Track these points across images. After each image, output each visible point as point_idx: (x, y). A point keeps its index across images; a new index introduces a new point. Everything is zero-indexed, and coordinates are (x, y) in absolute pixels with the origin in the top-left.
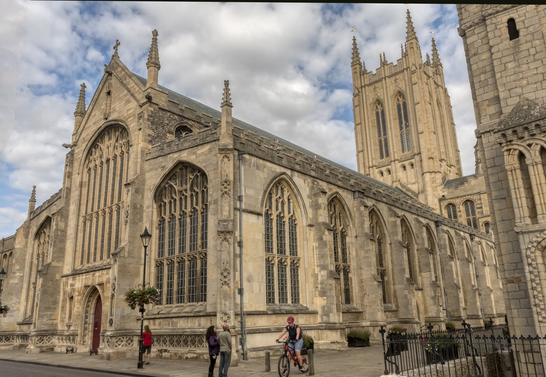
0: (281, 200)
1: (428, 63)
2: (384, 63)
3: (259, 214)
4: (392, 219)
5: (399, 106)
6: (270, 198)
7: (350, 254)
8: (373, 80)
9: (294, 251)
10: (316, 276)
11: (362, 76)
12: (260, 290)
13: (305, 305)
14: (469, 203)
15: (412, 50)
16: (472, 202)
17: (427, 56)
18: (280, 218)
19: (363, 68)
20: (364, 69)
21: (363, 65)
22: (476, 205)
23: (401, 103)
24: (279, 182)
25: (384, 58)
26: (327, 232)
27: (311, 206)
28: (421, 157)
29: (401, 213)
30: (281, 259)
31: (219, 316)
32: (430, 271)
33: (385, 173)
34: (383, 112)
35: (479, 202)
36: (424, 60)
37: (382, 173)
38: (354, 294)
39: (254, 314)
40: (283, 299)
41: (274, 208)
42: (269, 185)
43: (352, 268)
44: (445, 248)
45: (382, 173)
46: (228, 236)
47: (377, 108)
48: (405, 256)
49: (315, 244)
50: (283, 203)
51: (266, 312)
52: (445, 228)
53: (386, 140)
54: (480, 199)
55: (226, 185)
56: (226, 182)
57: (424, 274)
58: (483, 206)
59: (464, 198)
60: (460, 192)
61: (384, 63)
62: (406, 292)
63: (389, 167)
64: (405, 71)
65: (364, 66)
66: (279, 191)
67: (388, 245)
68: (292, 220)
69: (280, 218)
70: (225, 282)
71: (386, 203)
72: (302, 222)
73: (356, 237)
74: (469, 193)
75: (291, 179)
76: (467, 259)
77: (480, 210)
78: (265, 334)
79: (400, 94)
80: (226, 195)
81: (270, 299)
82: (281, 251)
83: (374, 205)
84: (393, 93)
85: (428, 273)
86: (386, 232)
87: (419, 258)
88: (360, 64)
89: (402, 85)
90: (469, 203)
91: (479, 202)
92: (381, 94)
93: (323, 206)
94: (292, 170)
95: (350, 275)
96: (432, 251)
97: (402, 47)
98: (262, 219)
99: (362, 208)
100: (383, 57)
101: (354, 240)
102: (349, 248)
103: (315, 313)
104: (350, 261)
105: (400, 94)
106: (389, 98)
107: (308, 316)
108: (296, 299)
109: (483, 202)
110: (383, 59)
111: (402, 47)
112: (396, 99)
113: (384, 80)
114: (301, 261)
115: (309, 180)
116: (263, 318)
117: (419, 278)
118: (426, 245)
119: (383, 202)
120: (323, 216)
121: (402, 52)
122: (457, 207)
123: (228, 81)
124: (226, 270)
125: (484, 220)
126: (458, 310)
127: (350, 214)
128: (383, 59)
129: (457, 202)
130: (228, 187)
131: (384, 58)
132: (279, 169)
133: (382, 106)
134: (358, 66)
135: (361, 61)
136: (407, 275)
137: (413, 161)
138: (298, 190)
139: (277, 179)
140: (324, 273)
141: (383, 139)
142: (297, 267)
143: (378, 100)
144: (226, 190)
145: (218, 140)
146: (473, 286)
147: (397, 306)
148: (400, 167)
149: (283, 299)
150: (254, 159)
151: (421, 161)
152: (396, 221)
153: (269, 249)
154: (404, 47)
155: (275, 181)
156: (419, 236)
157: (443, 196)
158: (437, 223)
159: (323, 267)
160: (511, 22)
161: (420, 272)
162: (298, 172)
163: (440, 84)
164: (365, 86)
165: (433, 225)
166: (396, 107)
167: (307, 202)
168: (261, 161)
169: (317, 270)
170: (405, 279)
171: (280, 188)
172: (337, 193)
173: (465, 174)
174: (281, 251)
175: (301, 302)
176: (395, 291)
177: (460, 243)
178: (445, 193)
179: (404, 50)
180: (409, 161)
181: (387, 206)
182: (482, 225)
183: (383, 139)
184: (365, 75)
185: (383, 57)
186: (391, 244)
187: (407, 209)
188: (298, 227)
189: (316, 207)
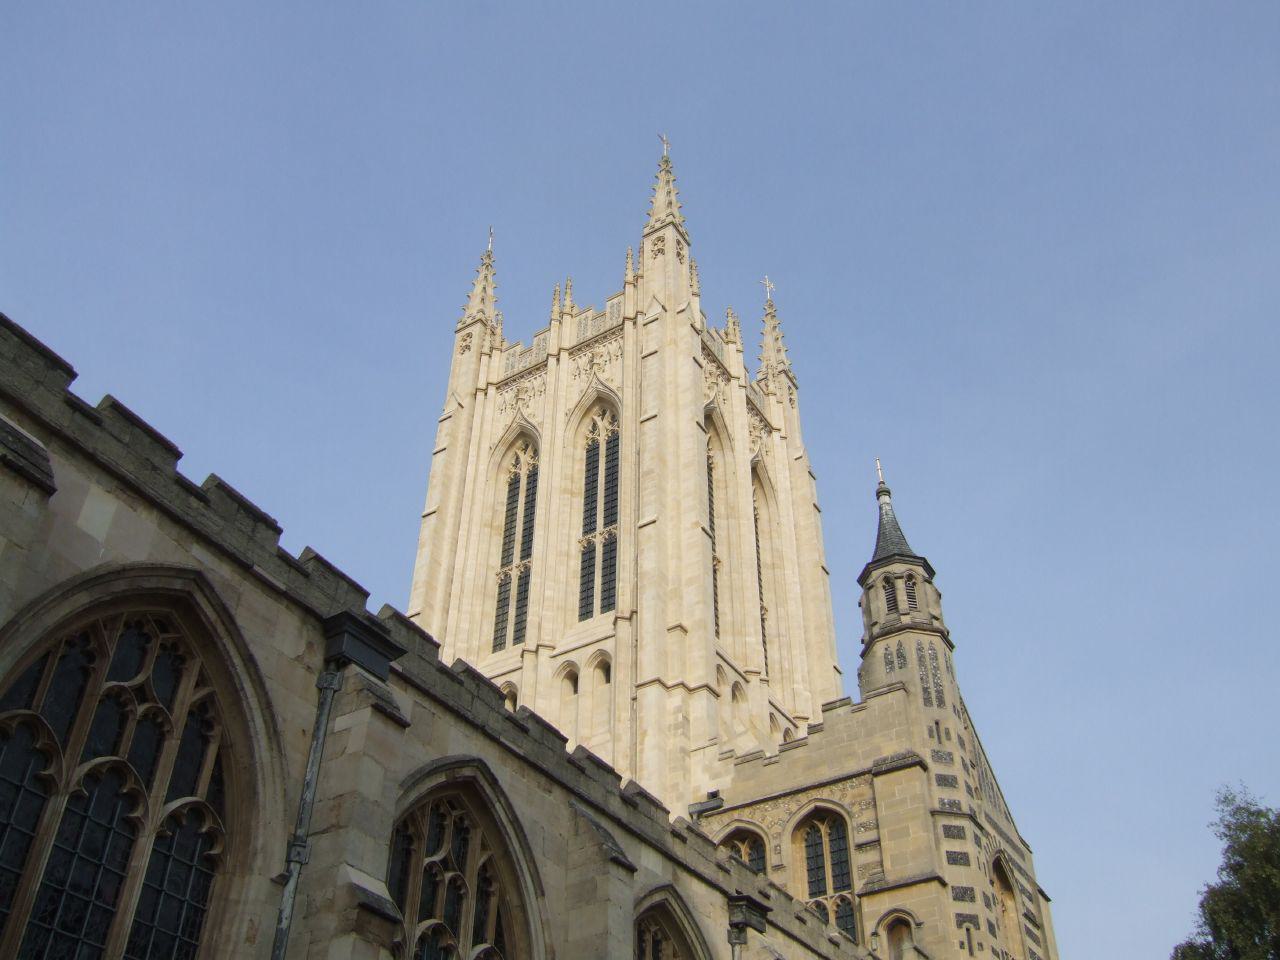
11: (485, 358)
14: (824, 829)
15: (660, 256)
22: (855, 837)
34: (533, 477)
35: (867, 816)
58: (884, 832)
59: (803, 798)
74: (827, 774)
77: (870, 856)
84: (576, 399)
90: (824, 829)
91: (867, 816)
109: (883, 812)
122: (769, 847)
125: (884, 904)
129: (777, 826)
148: (557, 674)
157: (714, 795)
182: (875, 934)
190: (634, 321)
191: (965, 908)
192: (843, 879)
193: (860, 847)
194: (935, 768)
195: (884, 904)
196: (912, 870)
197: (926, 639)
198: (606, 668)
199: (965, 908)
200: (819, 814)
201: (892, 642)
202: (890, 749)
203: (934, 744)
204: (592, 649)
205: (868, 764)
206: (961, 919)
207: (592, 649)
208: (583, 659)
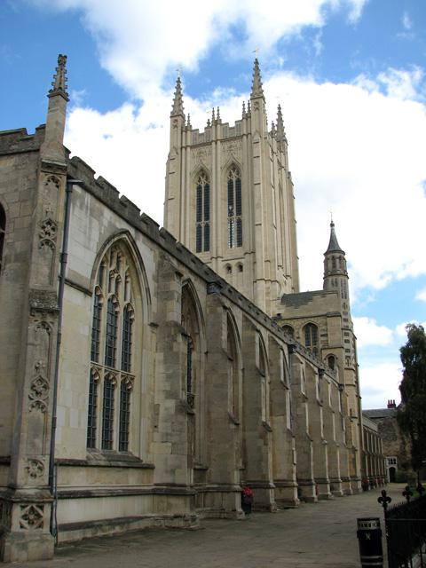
0: (116, 275)
3: (87, 292)
4: (249, 333)
5: (230, 183)
6: (102, 268)
7: (195, 378)
8: (200, 140)
9: (126, 365)
10: (156, 408)
11: (184, 133)
12: (79, 423)
13: (137, 455)
14: (311, 328)
15: (257, 111)
16: (315, 327)
17: (273, 124)
18: (113, 303)
19: (186, 122)
20: (189, 124)
21: (187, 119)
22: (320, 332)
23: (234, 180)
24: (115, 246)
25: (218, 114)
26: (180, 338)
27: (157, 294)
28: (254, 257)
30: (109, 375)
31: (22, 464)
32: (284, 414)
33: (235, 269)
35: (324, 328)
36: (269, 130)
37: (229, 268)
39: (79, 466)
40: (107, 443)
41: (105, 286)
42: (105, 245)
45: (229, 268)
46: (49, 319)
49: (160, 356)
50: (117, 283)
51: (86, 462)
53: (207, 227)
54: (326, 324)
55: (48, 228)
56: (49, 223)
58: (329, 333)
59: (306, 320)
60: (299, 312)
62: (261, 442)
63: (242, 261)
64: (245, 137)
65: (189, 121)
66: (115, 261)
68: (128, 312)
69: (113, 303)
70: (38, 403)
71: (242, 309)
72: (142, 319)
73: (206, 353)
74: (313, 314)
75: (134, 243)
76: (318, 402)
78: (83, 500)
79: (234, 167)
80: (46, 247)
81: (91, 443)
82: (110, 360)
85: (282, 417)
86: (239, 352)
87: (270, 393)
89: (240, 157)
90: (311, 328)
92: (209, 163)
93: (176, 295)
94: (138, 229)
97: (244, 105)
98: (91, 301)
99: (220, 309)
100: (216, 113)
102: (195, 370)
103: (150, 468)
104: (195, 390)
105: (234, 167)
106: (219, 169)
107: (140, 471)
108: (124, 444)
110: (216, 117)
111: (244, 105)
112: (228, 174)
114: (136, 381)
115: (158, 251)
116: (81, 473)
119: (238, 306)
120: (175, 312)
121: (244, 112)
123: (66, 57)
124: (41, 380)
125: (328, 352)
128: (216, 117)
129: (298, 326)
130: (52, 232)
131: (218, 114)
132: (125, 226)
133: (207, 178)
134: (179, 118)
137: (242, 261)
138: (142, 263)
139: (116, 239)
140: (171, 404)
141: (203, 225)
142: (129, 390)
143: (202, 170)
144: (47, 237)
145: (38, 151)
146: (322, 440)
149: (107, 443)
150: (88, 198)
151: (255, 263)
152: (254, 338)
153: (94, 356)
154: (246, 106)
155: (113, 241)
156: (274, 362)
157: (279, 315)
159: (170, 395)
162: (145, 234)
163: (283, 165)
164: (186, 149)
167: (152, 285)
168: (98, 205)
169: (159, 398)
170: (260, 424)
171: (115, 254)
172: (189, 280)
173: (304, 288)
174: (110, 360)
175: (130, 449)
179: (246, 110)
180: (237, 261)
181: (241, 312)
183: (203, 225)
184: (189, 132)
185: (216, 113)
188: (134, 324)
189: (165, 295)
190: (247, 136)
191: (347, 354)
192: (315, 341)
193: (322, 336)
194: (343, 317)
195: (328, 352)
196: (335, 344)
197: (343, 278)
198: (241, 268)
199: (347, 354)
200: (310, 324)
201: (334, 277)
202: (332, 310)
203: (343, 310)
205: (325, 313)
206: (347, 357)
207: (237, 261)
208: (233, 263)
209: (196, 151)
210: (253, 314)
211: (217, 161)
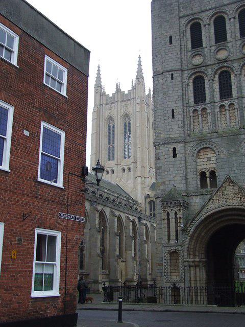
1: (149, 95)
2: (118, 90)
5: (125, 124)
28: (136, 164)
29: (117, 213)
34: (113, 126)
36: (147, 93)
38: (85, 264)
43: (85, 248)
44: (143, 235)
47: (110, 122)
48: (118, 241)
52: (144, 222)
53: (113, 147)
57: (128, 252)
61: (118, 90)
62: (116, 263)
67: (108, 234)
79: (126, 116)
83: (102, 209)
88: (101, 87)
89: (131, 110)
95: (84, 252)
96: (134, 238)
101: (88, 231)
105: (126, 116)
106: (119, 117)
113: (116, 103)
117: (124, 254)
118: (131, 234)
126: (146, 275)
127: (88, 215)
135: (102, 84)
136: (118, 253)
141: (111, 147)
147: (109, 272)
154: (134, 82)
158: (140, 219)
160: (174, 149)
161: (126, 250)
165: (137, 220)
166: (123, 125)
176: (109, 262)
177: (153, 232)
178: (150, 193)
179: (134, 84)
183: (111, 147)
186: (110, 233)
187: (122, 210)
204: (128, 166)
207: (128, 166)
208: (126, 168)
209: (107, 107)
210: (116, 208)
211: (117, 112)
